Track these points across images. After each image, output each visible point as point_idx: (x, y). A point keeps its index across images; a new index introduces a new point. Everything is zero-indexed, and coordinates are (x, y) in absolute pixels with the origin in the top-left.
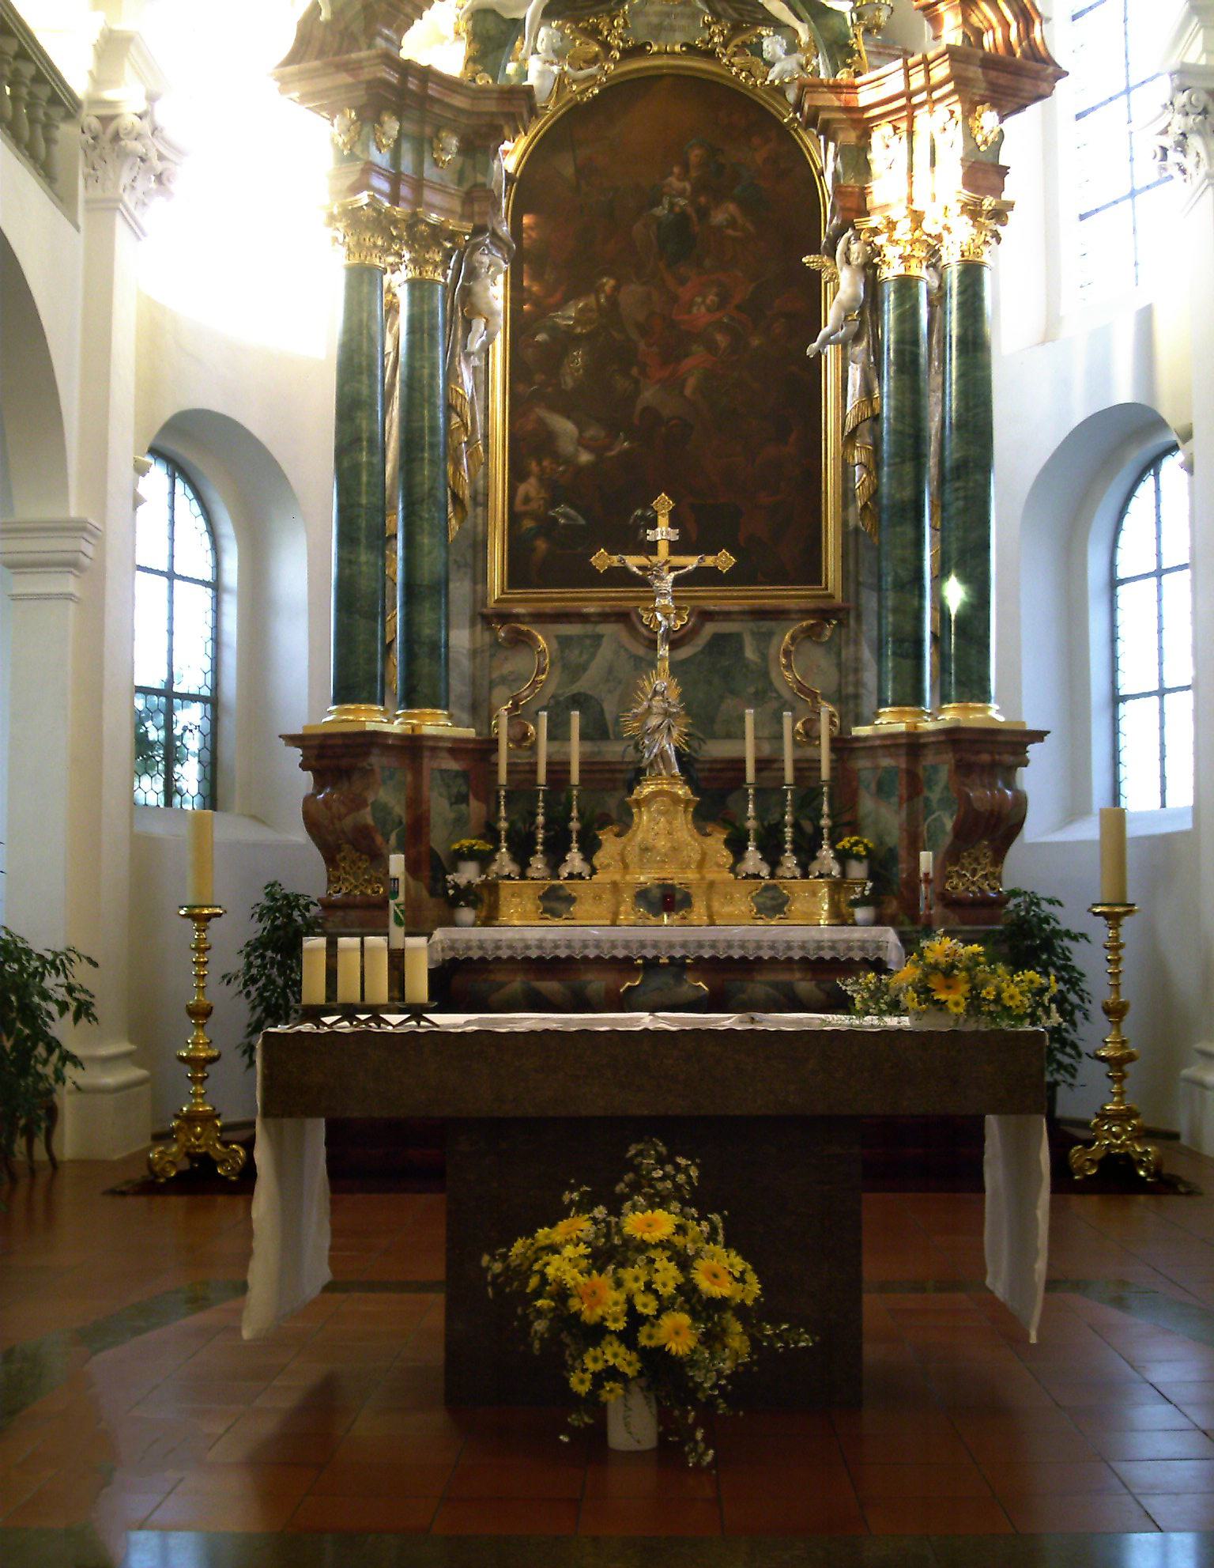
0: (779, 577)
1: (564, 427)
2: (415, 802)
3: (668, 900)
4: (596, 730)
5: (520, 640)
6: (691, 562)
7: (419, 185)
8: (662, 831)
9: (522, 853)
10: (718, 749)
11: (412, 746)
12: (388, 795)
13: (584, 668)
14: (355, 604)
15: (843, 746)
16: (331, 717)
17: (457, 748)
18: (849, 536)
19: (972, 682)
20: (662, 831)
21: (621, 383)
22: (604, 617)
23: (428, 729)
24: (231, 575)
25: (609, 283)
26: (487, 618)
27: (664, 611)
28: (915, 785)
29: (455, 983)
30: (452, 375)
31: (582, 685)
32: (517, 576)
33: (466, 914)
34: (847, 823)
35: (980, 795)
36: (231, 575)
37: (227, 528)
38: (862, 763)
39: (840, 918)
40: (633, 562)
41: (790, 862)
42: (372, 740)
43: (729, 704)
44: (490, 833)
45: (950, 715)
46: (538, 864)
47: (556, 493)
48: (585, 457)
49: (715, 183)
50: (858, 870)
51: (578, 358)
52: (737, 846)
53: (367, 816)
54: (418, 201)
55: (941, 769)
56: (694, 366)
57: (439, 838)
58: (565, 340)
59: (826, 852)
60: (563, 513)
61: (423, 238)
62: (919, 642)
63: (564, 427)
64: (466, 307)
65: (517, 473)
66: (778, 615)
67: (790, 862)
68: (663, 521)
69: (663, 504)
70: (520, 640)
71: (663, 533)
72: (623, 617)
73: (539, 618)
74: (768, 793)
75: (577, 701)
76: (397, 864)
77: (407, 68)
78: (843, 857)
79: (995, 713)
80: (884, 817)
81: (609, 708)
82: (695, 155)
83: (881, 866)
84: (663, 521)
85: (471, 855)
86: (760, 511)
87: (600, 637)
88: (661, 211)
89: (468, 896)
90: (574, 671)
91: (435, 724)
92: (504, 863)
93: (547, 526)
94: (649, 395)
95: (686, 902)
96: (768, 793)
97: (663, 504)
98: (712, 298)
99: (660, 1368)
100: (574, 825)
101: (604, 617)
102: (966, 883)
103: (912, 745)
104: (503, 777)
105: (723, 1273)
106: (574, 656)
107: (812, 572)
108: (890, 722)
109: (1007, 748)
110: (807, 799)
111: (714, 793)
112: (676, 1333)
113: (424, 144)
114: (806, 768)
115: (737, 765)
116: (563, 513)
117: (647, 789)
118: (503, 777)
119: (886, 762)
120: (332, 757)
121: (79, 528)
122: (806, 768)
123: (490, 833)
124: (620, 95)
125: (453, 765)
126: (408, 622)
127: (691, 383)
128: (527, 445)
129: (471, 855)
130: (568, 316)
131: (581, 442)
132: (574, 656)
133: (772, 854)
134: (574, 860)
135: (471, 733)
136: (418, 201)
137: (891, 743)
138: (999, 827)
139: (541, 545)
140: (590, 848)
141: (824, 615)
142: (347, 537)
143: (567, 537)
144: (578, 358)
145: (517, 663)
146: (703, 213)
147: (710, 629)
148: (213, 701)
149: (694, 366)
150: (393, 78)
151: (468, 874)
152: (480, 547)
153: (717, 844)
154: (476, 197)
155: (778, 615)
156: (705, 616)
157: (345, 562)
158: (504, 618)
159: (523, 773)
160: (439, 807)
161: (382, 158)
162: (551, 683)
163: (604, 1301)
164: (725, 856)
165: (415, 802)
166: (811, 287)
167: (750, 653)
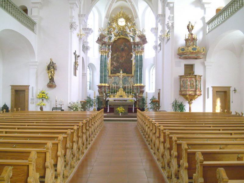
0: (129, 73)
1: (114, 63)
2: (105, 90)
3: (121, 96)
4: (117, 84)
5: (111, 78)
6: (123, 74)
7: (105, 49)
8: (121, 92)
9: (112, 93)
10: (125, 86)
11: (105, 86)
12: (103, 90)
13: (116, 80)
14: (101, 77)
15: (133, 86)
16: (100, 84)
17: (108, 86)
18: (134, 71)
19: (141, 82)
20: (121, 92)
21: (118, 60)
22: (117, 76)
23: (106, 85)
24: (91, 73)
25: (118, 53)
26: (109, 76)
27: (121, 77)
28: (137, 89)
29: (114, 101)
30: (107, 61)
31: (116, 81)
32: (111, 73)
33: (108, 97)
34: (133, 91)
35: (141, 90)
36: (91, 73)
37: (91, 70)
38: (134, 87)
39: (132, 98)
40: (119, 74)
41: (129, 94)
42: (102, 86)
43: (126, 83)
44: (110, 92)
45: (138, 84)
46: (113, 94)
47: (114, 68)
48: (116, 65)
49: (125, 46)
50: (134, 94)
51: (115, 58)
52: (126, 93)
53: (102, 91)
54: (105, 50)
55: (139, 88)
56: (123, 59)
57: (107, 92)
58: (114, 57)
59: (131, 93)
60: (114, 69)
61: (105, 52)
62: (138, 80)
63: (114, 63)
64: (108, 56)
65: (111, 66)
66: (129, 76)
67: (129, 94)
68: (121, 71)
69: (121, 70)
70: (111, 78)
71: (121, 72)
72: (118, 76)
73: (113, 76)
74: (128, 89)
75: (115, 82)
76: (104, 94)
77: (105, 42)
78: (133, 94)
79: (142, 85)
80: (135, 91)
81: (117, 83)
82: (124, 43)
83: (135, 94)
84: (121, 71)
85: (109, 93)
86: (128, 70)
87: (116, 78)
88: (121, 48)
89: (108, 96)
90: (115, 80)
91: (107, 85)
92: (111, 94)
93: (113, 70)
94: (120, 61)
95: (122, 97)
96: (128, 89)
97: (121, 70)
98: (125, 54)
99: (121, 112)
100: (115, 91)
101: (117, 76)
102: (140, 95)
103: (137, 86)
104: (111, 88)
105: (124, 109)
106: (115, 79)
107: (131, 73)
108: (136, 85)
109: (143, 87)
110: (130, 90)
111: (124, 89)
112: (122, 111)
113: (106, 46)
114: (130, 87)
115: (126, 87)
116: (114, 69)
117: (120, 89)
118: (111, 88)
119: (136, 87)
120: (100, 87)
121: (86, 74)
122: (130, 87)
123: (110, 92)
124: (119, 39)
125: (107, 87)
126: (105, 78)
127: (123, 60)
128: (112, 64)
129: (109, 93)
130: (115, 55)
131: (116, 64)
132: (115, 79)
133: (128, 93)
134: (115, 93)
135: (108, 85)
136: (105, 50)
137: (136, 86)
138: (142, 92)
139: (113, 71)
140: (116, 93)
141: (132, 76)
142: (101, 72)
143: (115, 71)
144: (115, 58)
145: (111, 79)
146: (124, 48)
147: (124, 77)
148: (90, 82)
149: (123, 59)
150: (104, 43)
151: (108, 95)
152: (108, 71)
153: (125, 92)
154: (109, 49)
155: (129, 76)
156: (124, 76)
157: (100, 74)
158: (110, 76)
159: (112, 87)
160: (107, 90)
161: (103, 47)
162: (113, 81)
163: (120, 110)
164: (125, 93)
165: (105, 90)
166: (132, 56)
167: (127, 79)
